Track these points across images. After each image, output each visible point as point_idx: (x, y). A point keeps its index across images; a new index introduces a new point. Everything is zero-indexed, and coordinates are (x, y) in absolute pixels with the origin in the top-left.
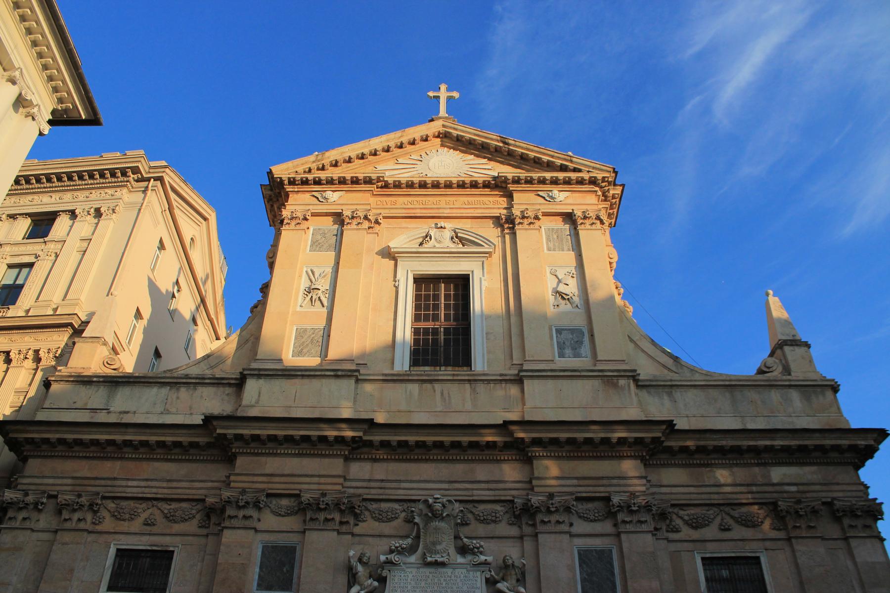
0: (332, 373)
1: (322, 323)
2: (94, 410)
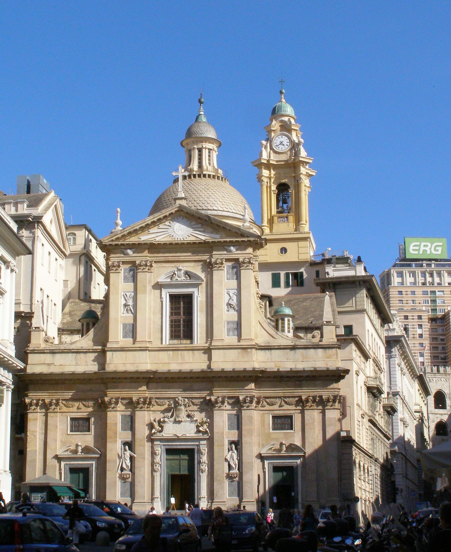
0: (139, 349)
1: (132, 322)
2: (49, 364)
